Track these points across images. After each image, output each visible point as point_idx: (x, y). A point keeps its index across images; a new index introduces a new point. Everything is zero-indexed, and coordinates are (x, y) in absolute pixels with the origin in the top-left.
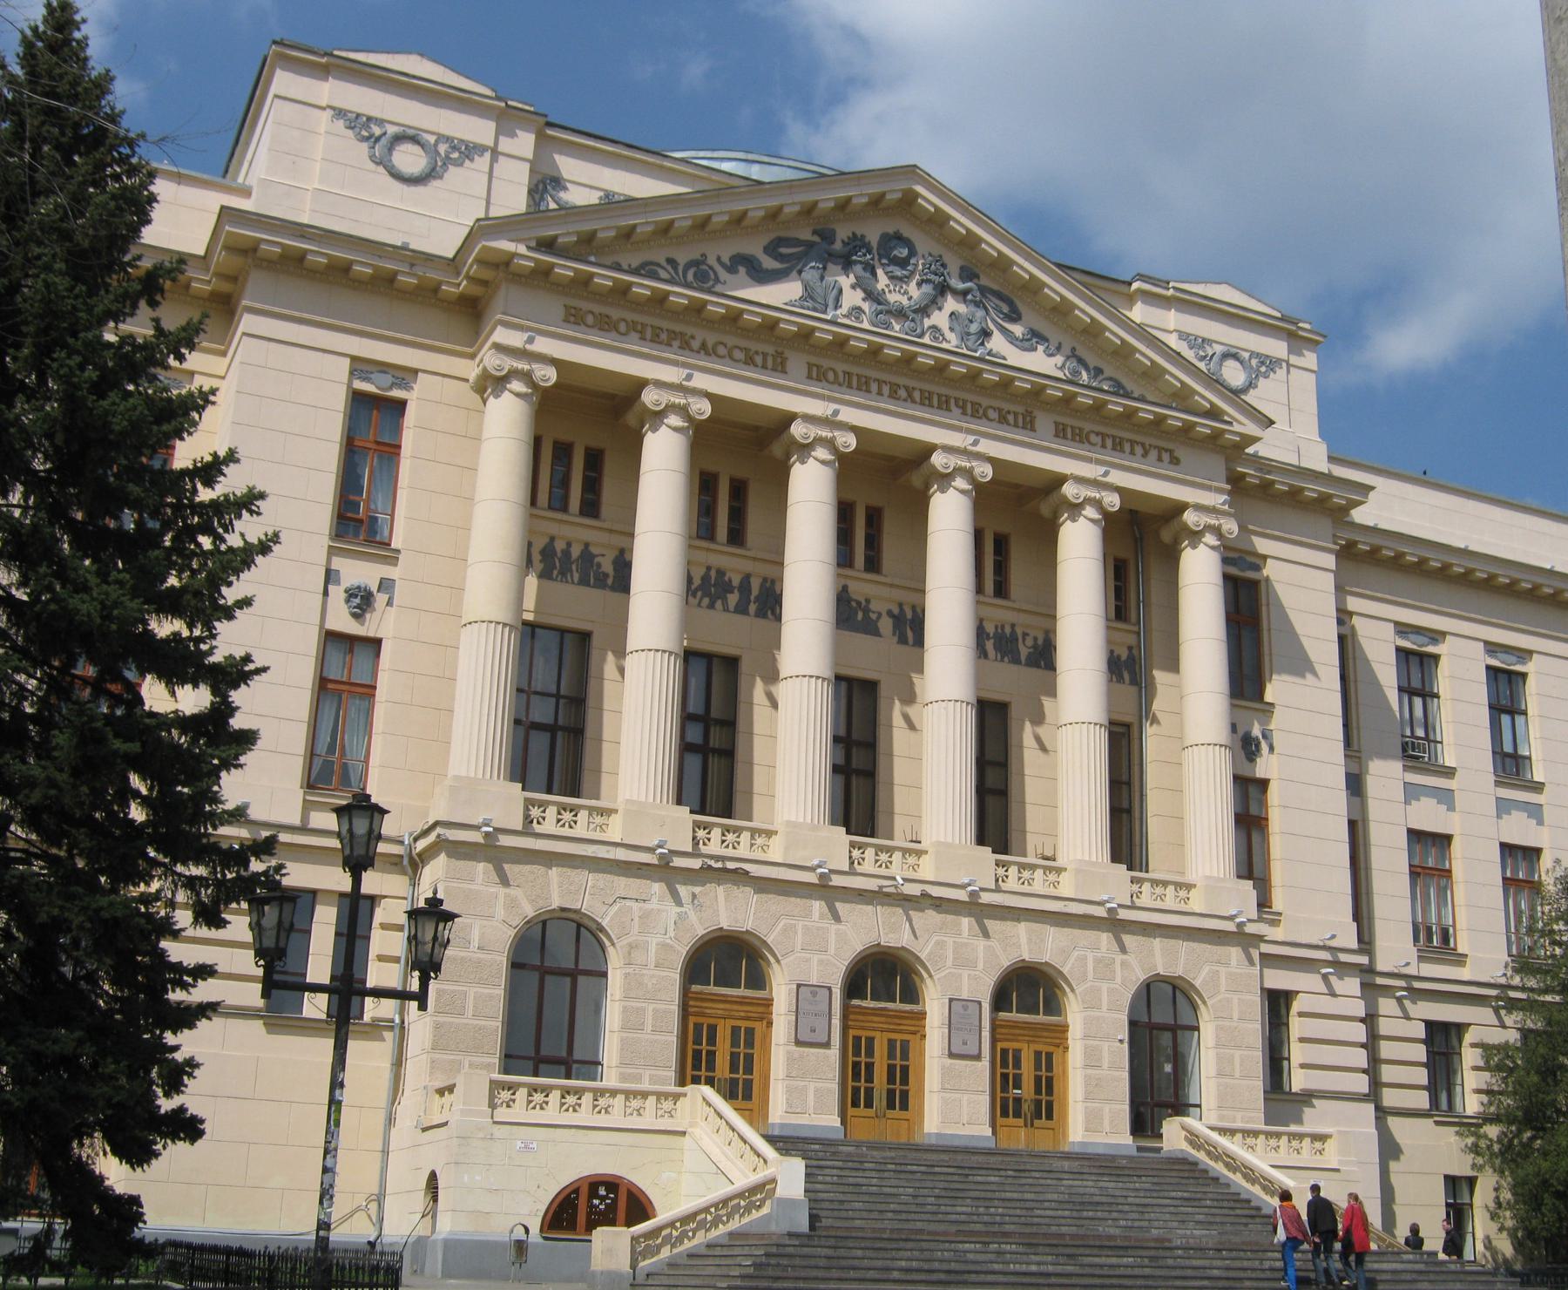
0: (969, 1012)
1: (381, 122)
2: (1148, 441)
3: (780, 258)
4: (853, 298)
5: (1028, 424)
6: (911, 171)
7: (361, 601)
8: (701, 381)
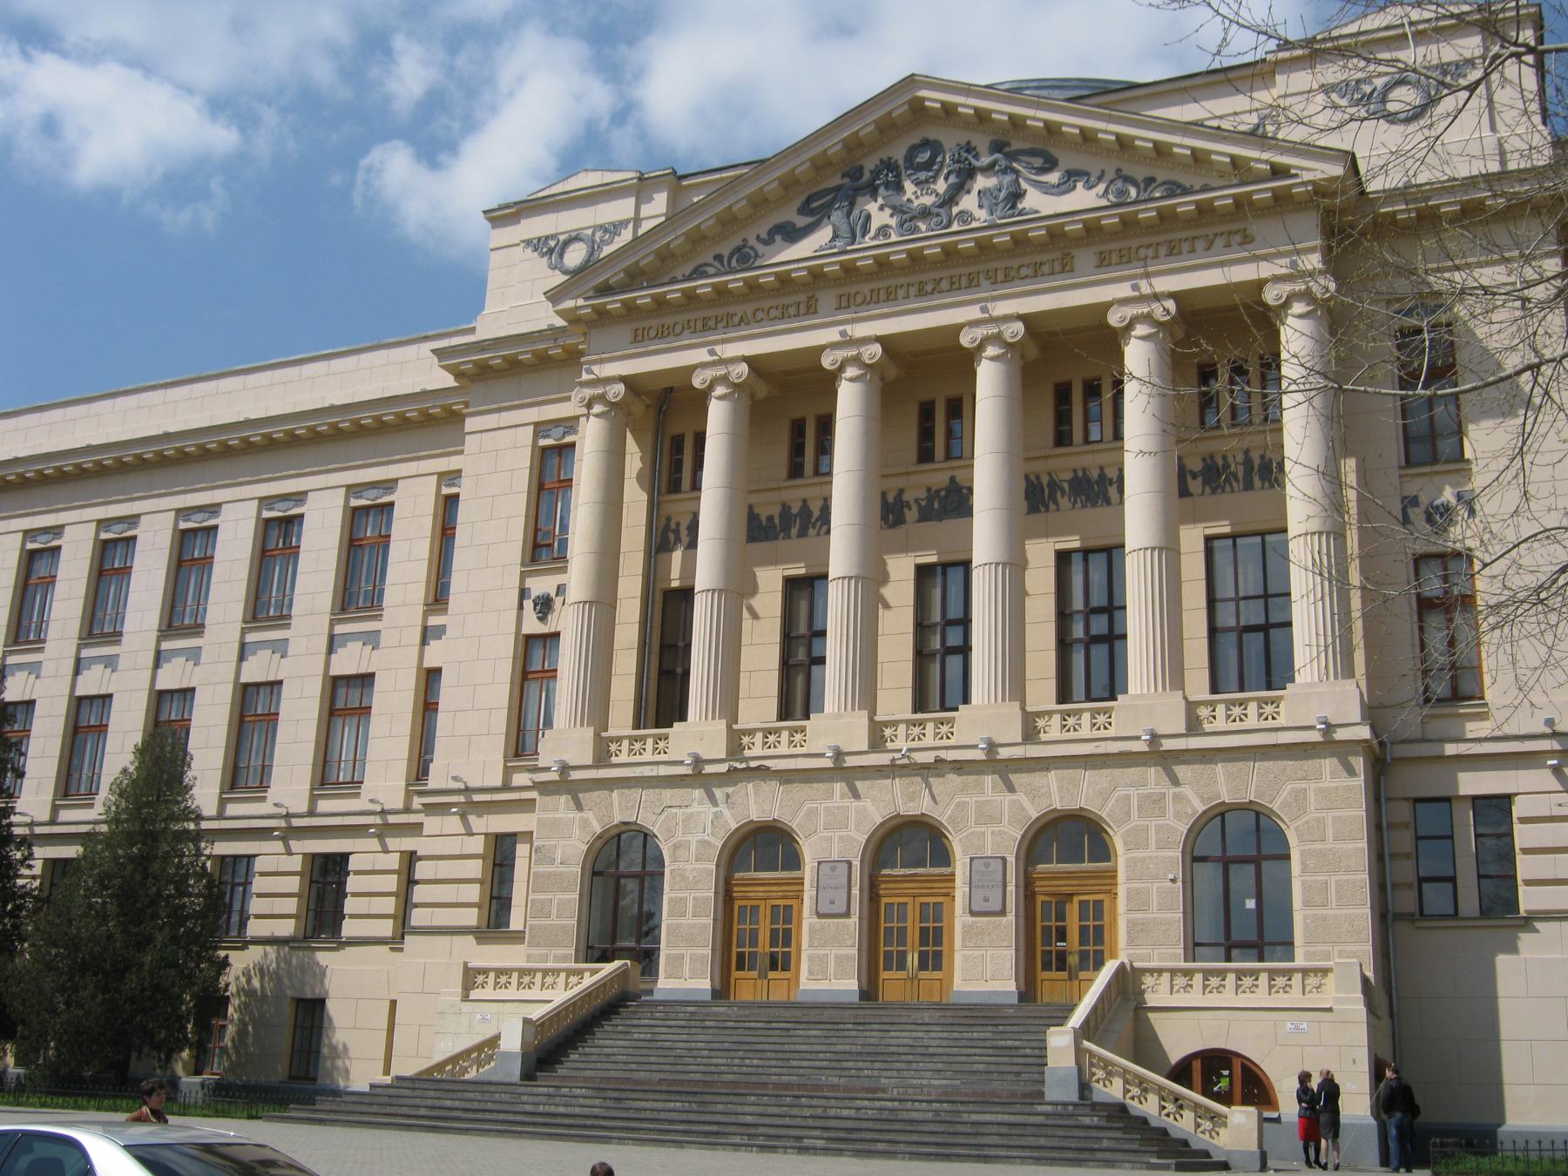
0: (991, 868)
1: (553, 237)
2: (1210, 231)
3: (812, 213)
5: (1066, 267)
6: (910, 81)
8: (1001, 308)
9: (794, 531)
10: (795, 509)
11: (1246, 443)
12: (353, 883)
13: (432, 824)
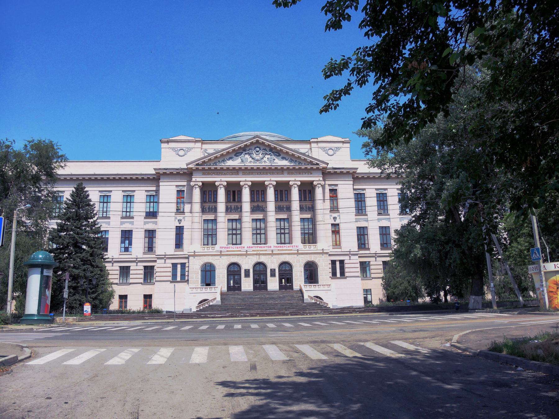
4: (250, 159)
7: (180, 221)
9: (229, 211)
10: (229, 207)
11: (306, 204)
12: (131, 272)
13: (158, 261)
